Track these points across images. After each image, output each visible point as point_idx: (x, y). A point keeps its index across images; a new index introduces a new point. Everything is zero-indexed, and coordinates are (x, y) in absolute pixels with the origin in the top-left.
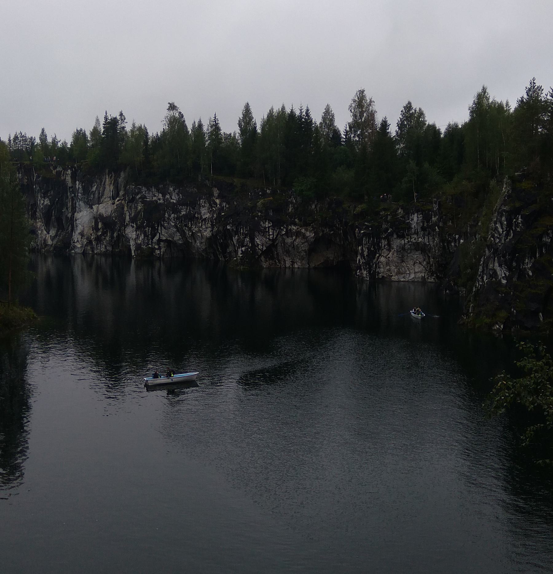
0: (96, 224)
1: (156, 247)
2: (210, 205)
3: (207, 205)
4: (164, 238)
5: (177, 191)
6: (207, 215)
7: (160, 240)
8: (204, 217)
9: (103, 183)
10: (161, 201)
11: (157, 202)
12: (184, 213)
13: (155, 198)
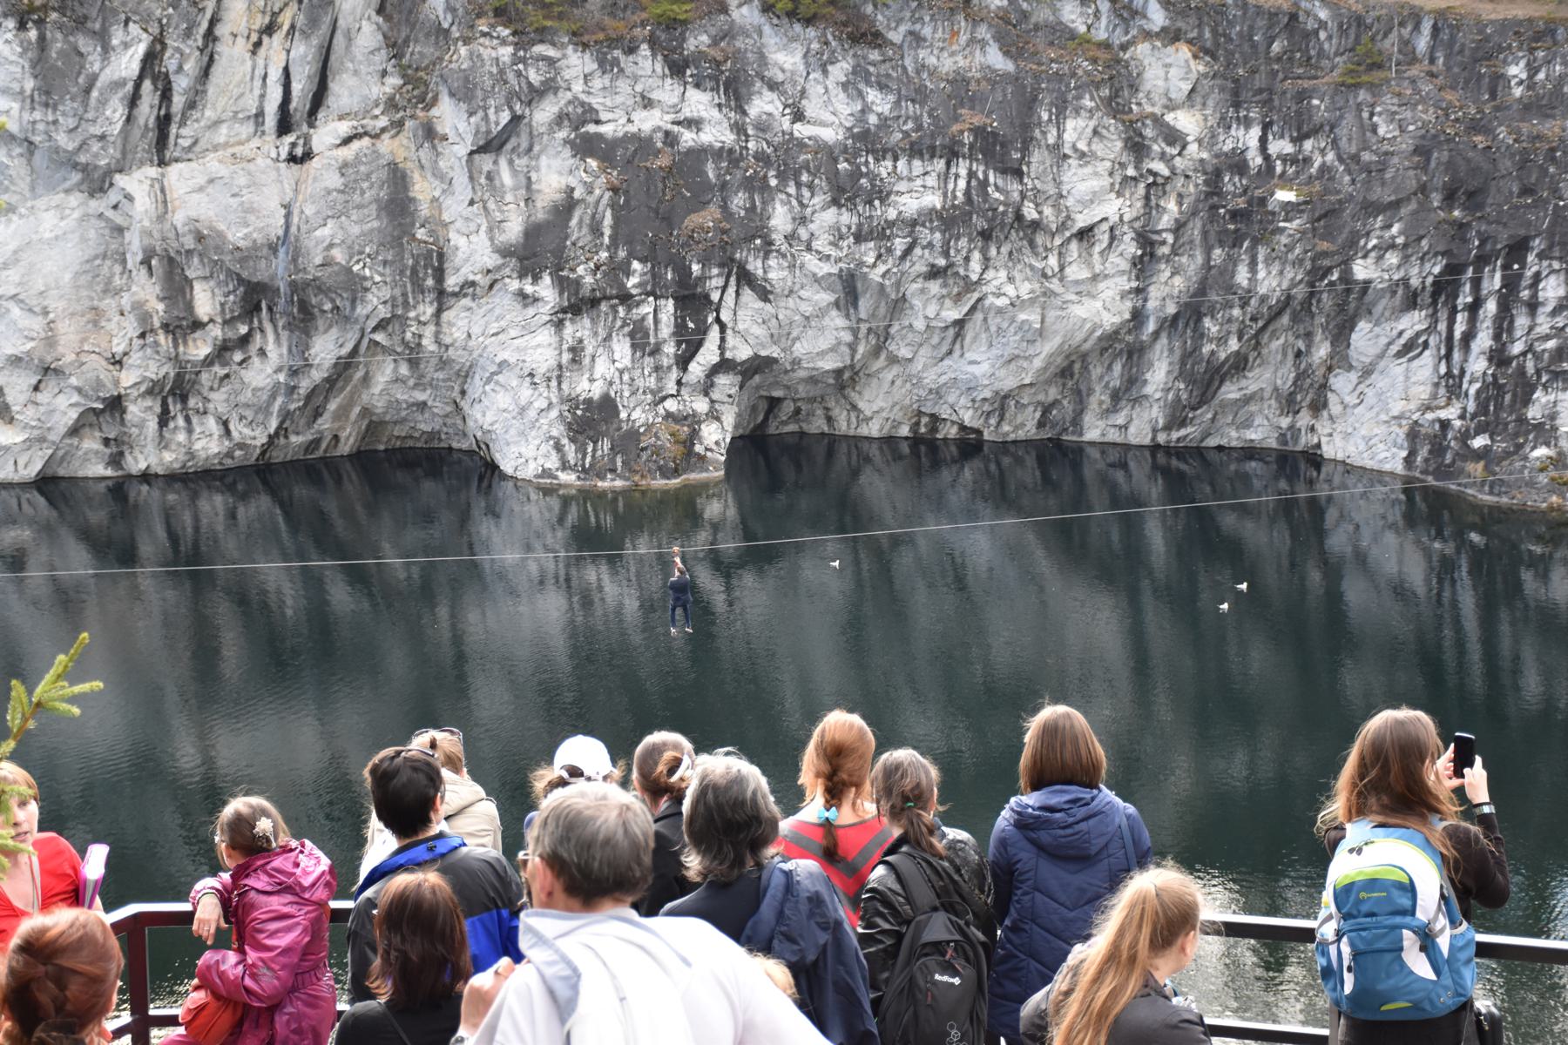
0: (177, 288)
1: (701, 406)
2: (1137, 147)
3: (1113, 146)
4: (741, 352)
5: (839, 71)
6: (1112, 208)
7: (724, 365)
8: (1081, 221)
9: (205, 25)
10: (716, 133)
11: (670, 139)
12: (934, 200)
13: (648, 122)
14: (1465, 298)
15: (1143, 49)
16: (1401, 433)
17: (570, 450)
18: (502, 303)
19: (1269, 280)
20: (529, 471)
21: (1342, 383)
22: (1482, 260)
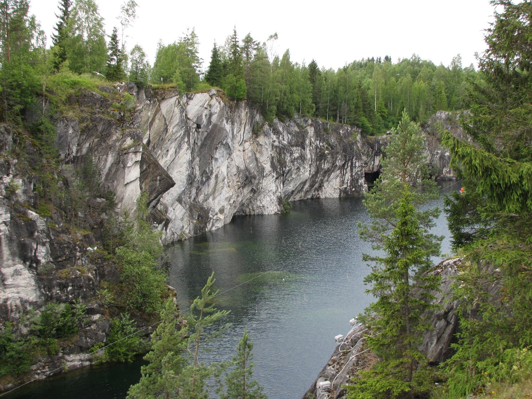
14: (346, 167)
15: (308, 128)
16: (339, 191)
17: (278, 207)
18: (270, 177)
19: (326, 166)
20: (273, 213)
21: (325, 184)
22: (349, 160)
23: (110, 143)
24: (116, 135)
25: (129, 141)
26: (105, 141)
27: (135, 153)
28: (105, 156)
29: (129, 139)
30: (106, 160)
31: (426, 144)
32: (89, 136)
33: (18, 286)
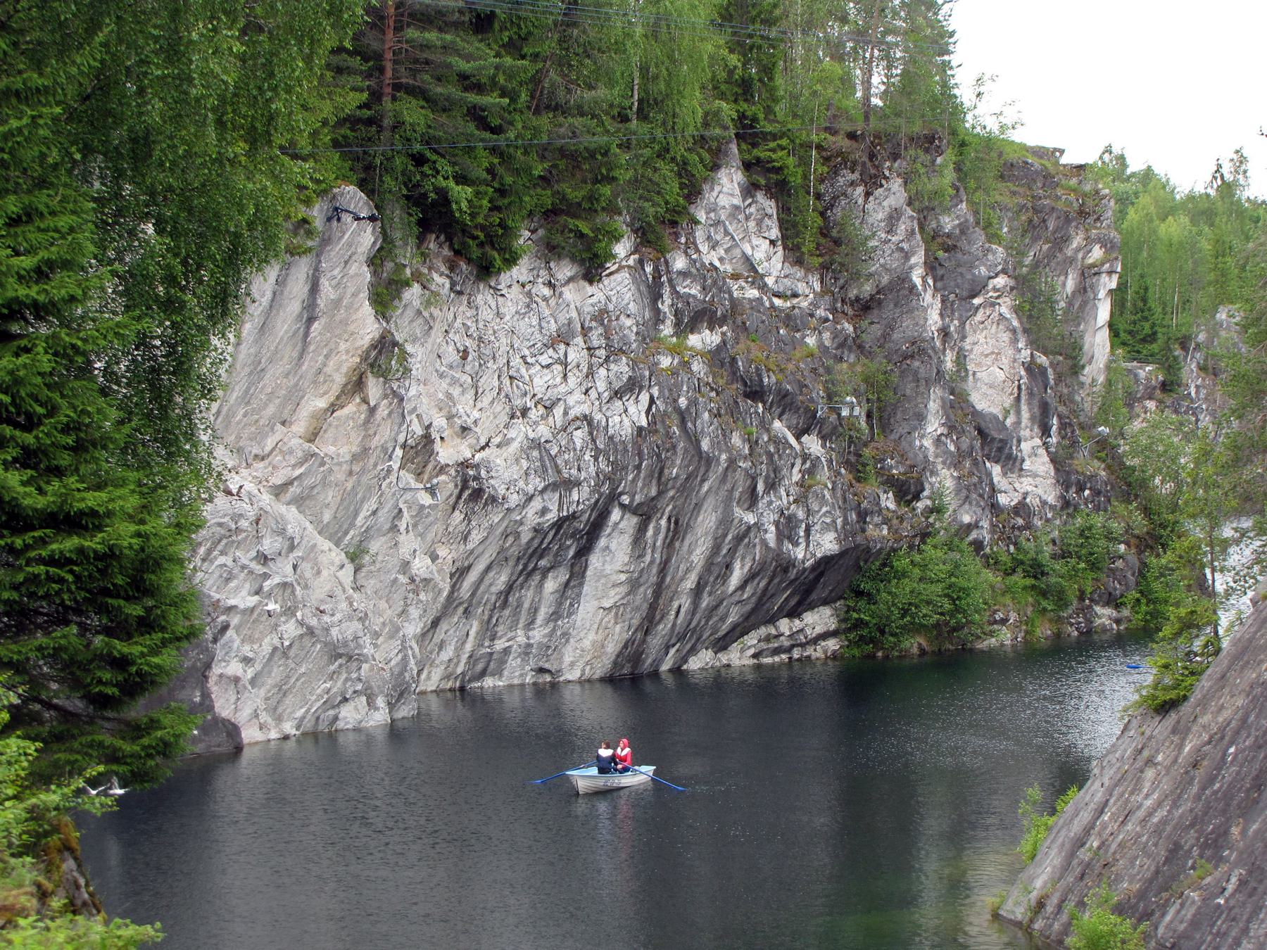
23: (1069, 253)
24: (1077, 241)
25: (1097, 253)
26: (1061, 250)
27: (1110, 273)
28: (1062, 278)
29: (1097, 247)
30: (1064, 285)
31: (1202, 396)
32: (1035, 239)
33: (1035, 476)
